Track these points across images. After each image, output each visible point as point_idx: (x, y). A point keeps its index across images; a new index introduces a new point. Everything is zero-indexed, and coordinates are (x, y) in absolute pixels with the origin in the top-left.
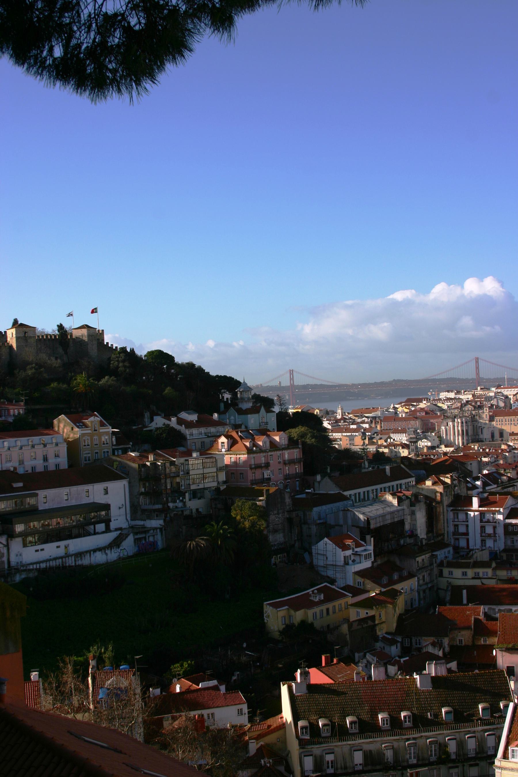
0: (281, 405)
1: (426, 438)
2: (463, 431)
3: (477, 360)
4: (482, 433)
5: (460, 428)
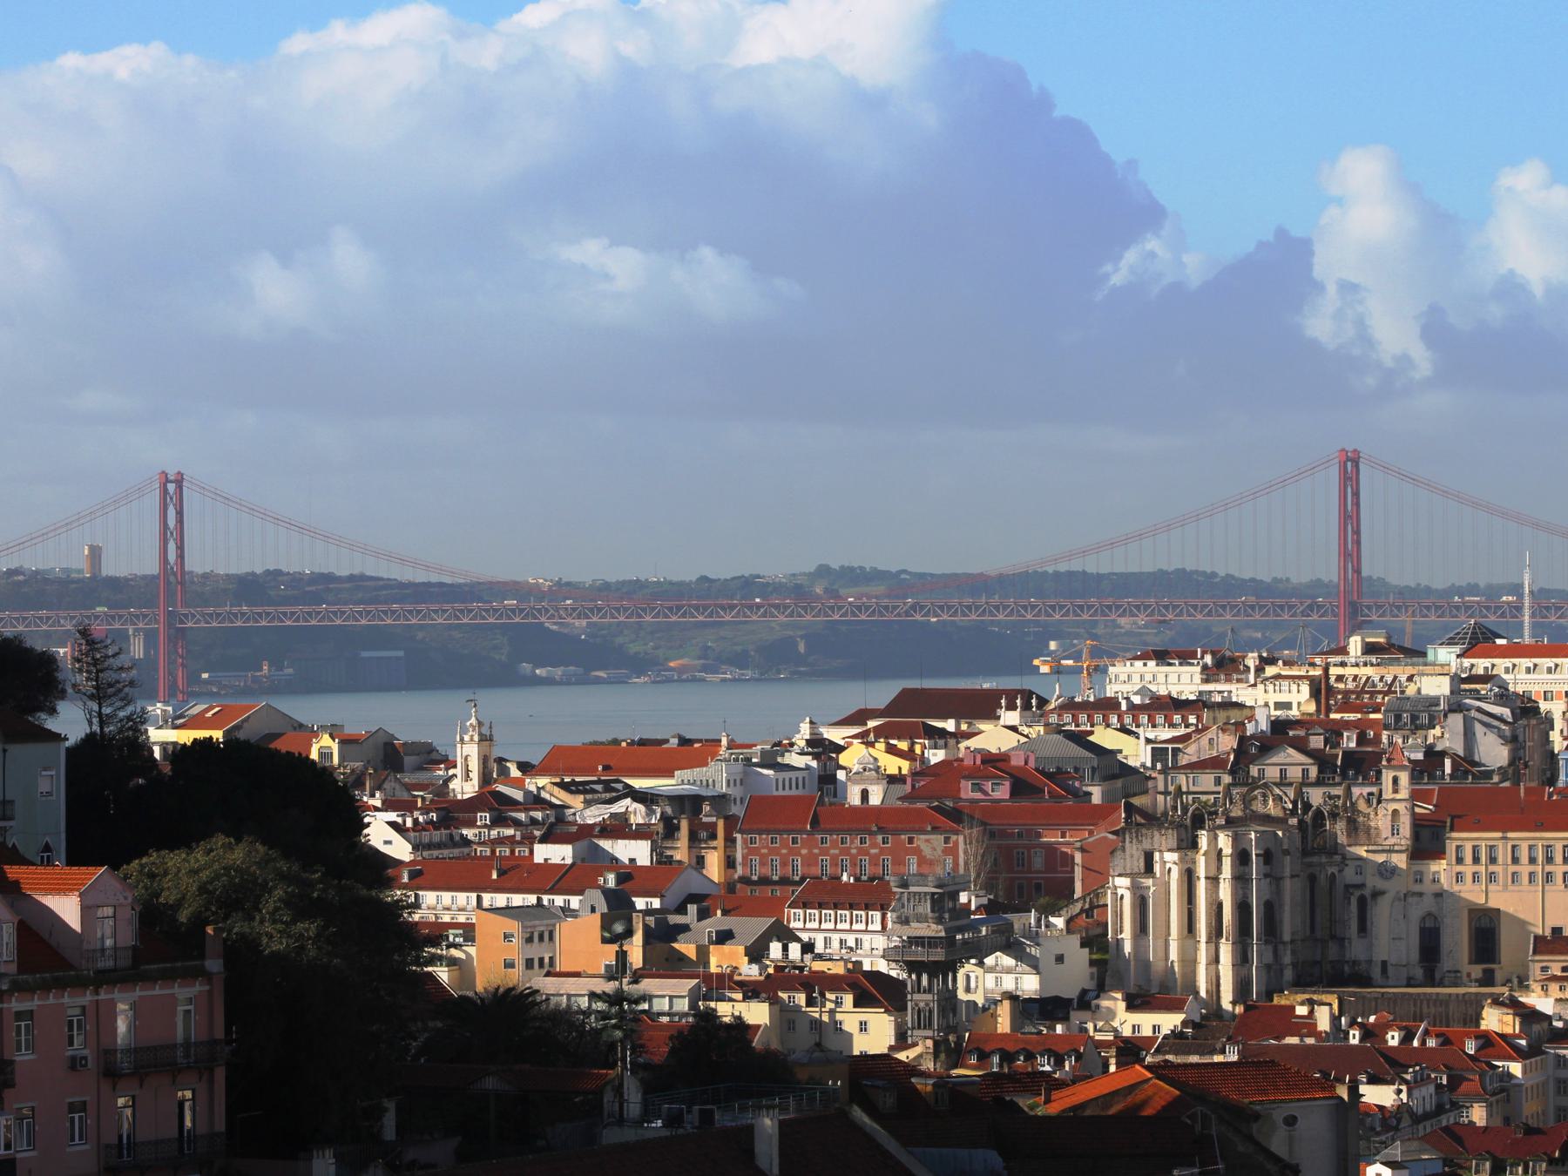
0: (100, 694)
1: (1012, 947)
2: (1242, 908)
3: (1350, 467)
4: (1363, 928)
5: (1225, 893)
